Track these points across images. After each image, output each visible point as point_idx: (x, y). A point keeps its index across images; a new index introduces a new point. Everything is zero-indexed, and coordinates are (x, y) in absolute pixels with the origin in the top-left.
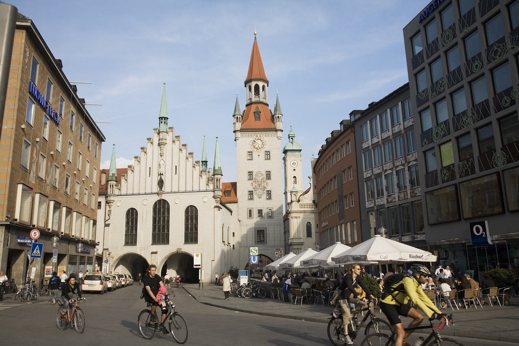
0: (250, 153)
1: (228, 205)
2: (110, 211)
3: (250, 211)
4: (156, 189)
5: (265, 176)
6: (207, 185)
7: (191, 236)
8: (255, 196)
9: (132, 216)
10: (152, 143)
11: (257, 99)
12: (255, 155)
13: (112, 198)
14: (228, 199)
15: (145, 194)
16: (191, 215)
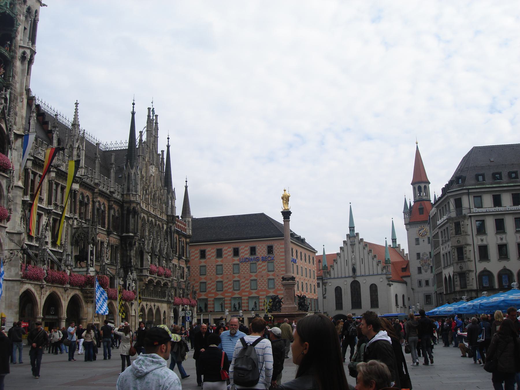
0: (417, 240)
1: (405, 279)
2: (325, 289)
3: (420, 282)
4: (351, 274)
5: (429, 256)
6: (382, 270)
7: (374, 303)
8: (423, 271)
9: (338, 290)
10: (347, 244)
11: (420, 197)
12: (421, 240)
13: (326, 281)
14: (404, 274)
15: (345, 277)
16: (373, 289)
